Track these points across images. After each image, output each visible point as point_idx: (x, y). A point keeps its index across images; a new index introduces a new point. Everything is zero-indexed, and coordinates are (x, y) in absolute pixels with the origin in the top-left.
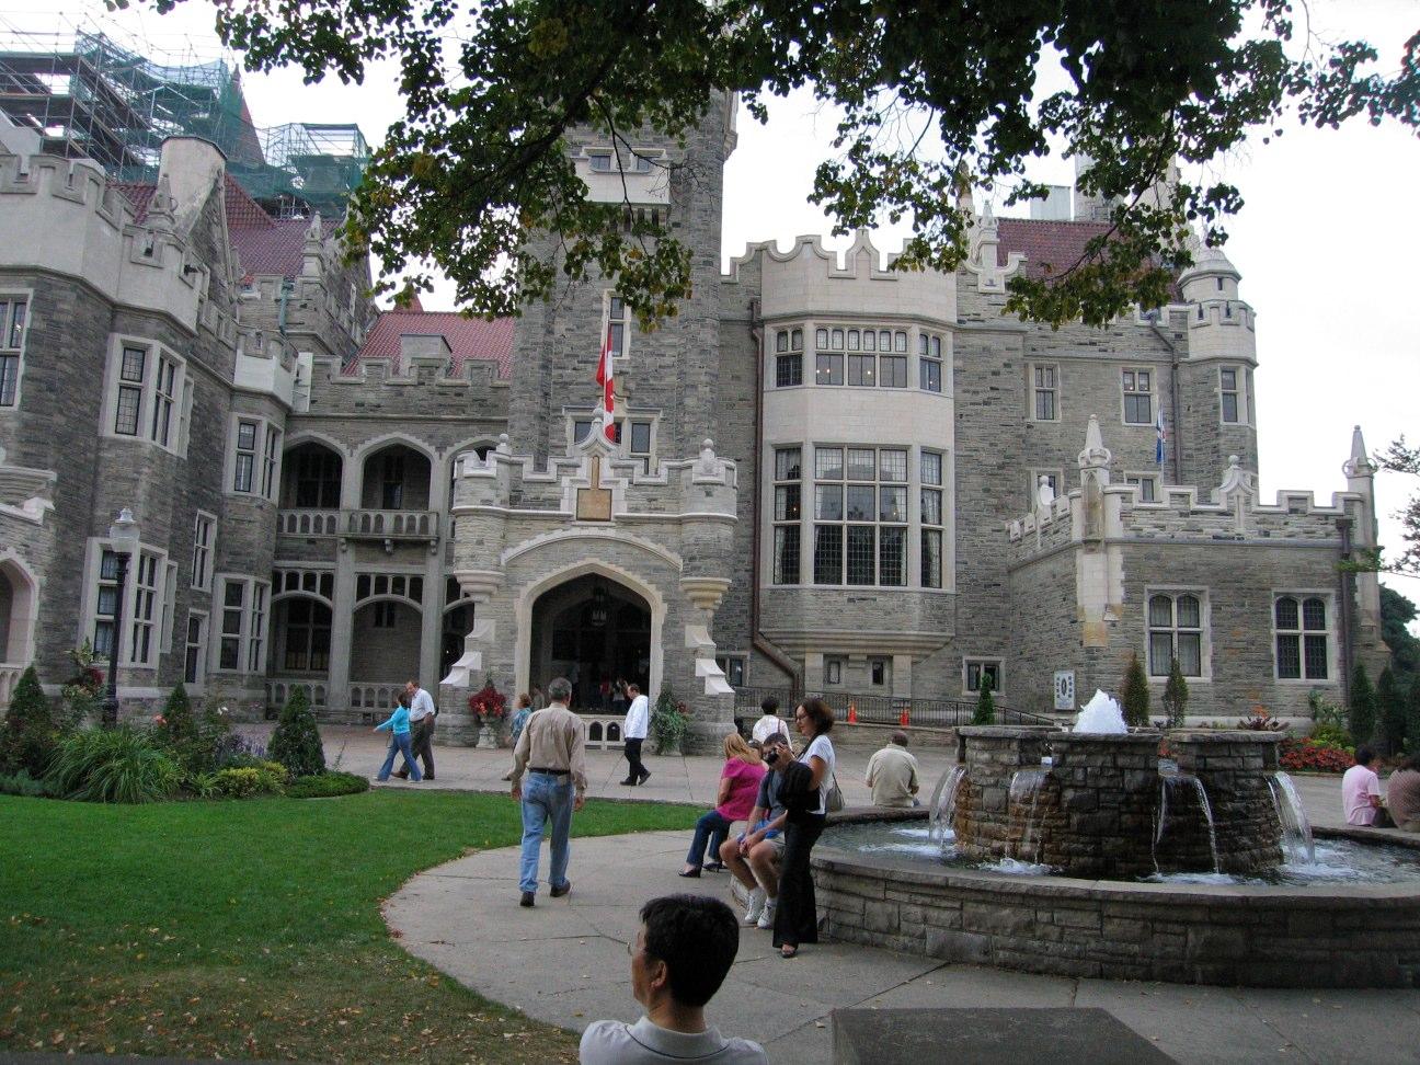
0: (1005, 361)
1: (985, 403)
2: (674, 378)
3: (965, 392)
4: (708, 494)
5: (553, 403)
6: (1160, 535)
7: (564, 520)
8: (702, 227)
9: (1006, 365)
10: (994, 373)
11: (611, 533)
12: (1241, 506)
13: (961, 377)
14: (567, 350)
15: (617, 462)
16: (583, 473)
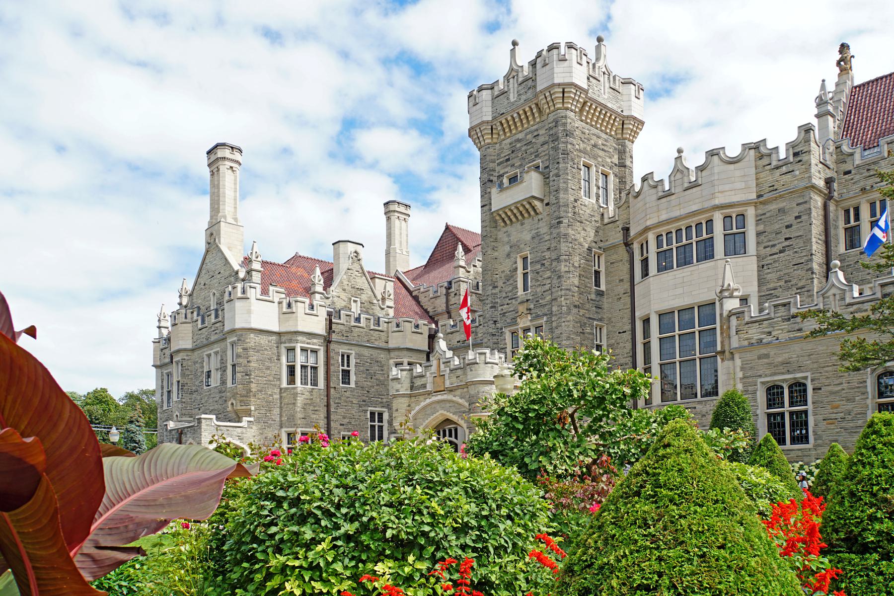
0: (797, 214)
1: (781, 252)
2: (550, 297)
3: (765, 248)
4: (471, 370)
5: (499, 325)
6: (766, 339)
7: (429, 394)
8: (555, 202)
9: (797, 218)
10: (788, 227)
11: (445, 397)
12: (837, 302)
13: (762, 237)
14: (504, 295)
15: (445, 360)
16: (434, 369)
